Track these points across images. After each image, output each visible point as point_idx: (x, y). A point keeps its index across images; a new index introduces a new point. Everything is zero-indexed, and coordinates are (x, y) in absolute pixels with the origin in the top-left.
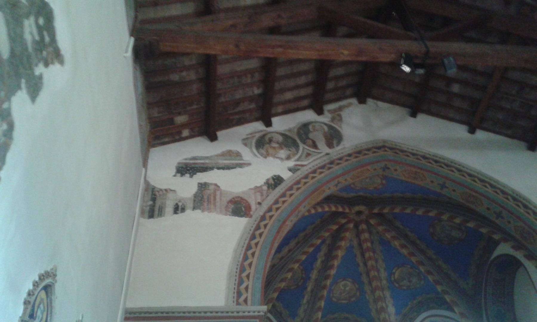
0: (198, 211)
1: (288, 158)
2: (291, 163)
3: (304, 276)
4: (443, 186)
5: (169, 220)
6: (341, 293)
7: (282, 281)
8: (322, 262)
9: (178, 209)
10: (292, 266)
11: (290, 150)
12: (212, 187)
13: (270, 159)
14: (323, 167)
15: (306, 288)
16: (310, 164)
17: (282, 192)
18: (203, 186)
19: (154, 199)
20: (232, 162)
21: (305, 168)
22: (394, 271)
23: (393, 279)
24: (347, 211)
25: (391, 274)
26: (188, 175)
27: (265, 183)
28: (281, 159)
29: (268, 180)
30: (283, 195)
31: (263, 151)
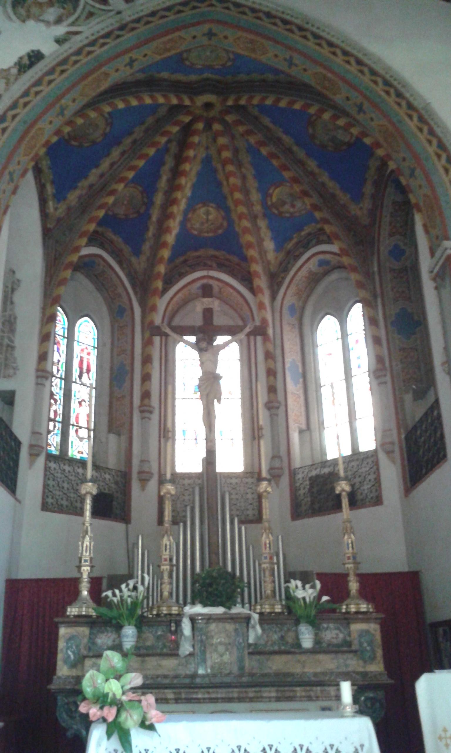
1: (59, 21)
2: (61, 30)
3: (146, 200)
4: (291, 63)
6: (202, 224)
7: (101, 207)
8: (168, 181)
10: (115, 186)
11: (64, 8)
13: (31, 23)
14: (107, 35)
15: (149, 217)
16: (90, 30)
17: (37, 77)
21: (78, 38)
22: (271, 191)
23: (269, 203)
24: (187, 102)
25: (266, 195)
27: (15, 64)
28: (48, 23)
29: (21, 58)
30: (38, 83)
31: (22, 11)
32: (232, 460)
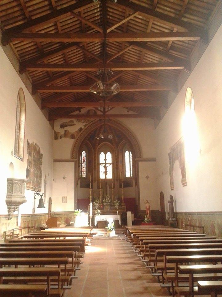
0: (65, 138)
1: (84, 122)
2: (84, 124)
5: (59, 140)
9: (61, 137)
12: (68, 131)
18: (66, 131)
19: (56, 135)
20: (71, 124)
26: (62, 128)
32: (110, 176)
